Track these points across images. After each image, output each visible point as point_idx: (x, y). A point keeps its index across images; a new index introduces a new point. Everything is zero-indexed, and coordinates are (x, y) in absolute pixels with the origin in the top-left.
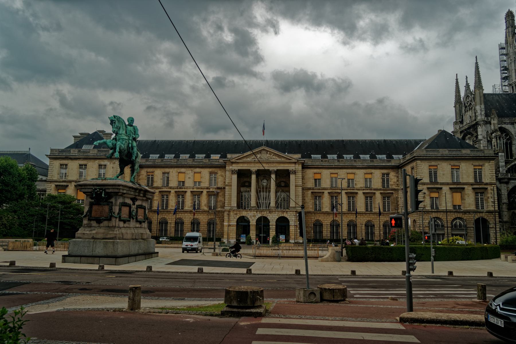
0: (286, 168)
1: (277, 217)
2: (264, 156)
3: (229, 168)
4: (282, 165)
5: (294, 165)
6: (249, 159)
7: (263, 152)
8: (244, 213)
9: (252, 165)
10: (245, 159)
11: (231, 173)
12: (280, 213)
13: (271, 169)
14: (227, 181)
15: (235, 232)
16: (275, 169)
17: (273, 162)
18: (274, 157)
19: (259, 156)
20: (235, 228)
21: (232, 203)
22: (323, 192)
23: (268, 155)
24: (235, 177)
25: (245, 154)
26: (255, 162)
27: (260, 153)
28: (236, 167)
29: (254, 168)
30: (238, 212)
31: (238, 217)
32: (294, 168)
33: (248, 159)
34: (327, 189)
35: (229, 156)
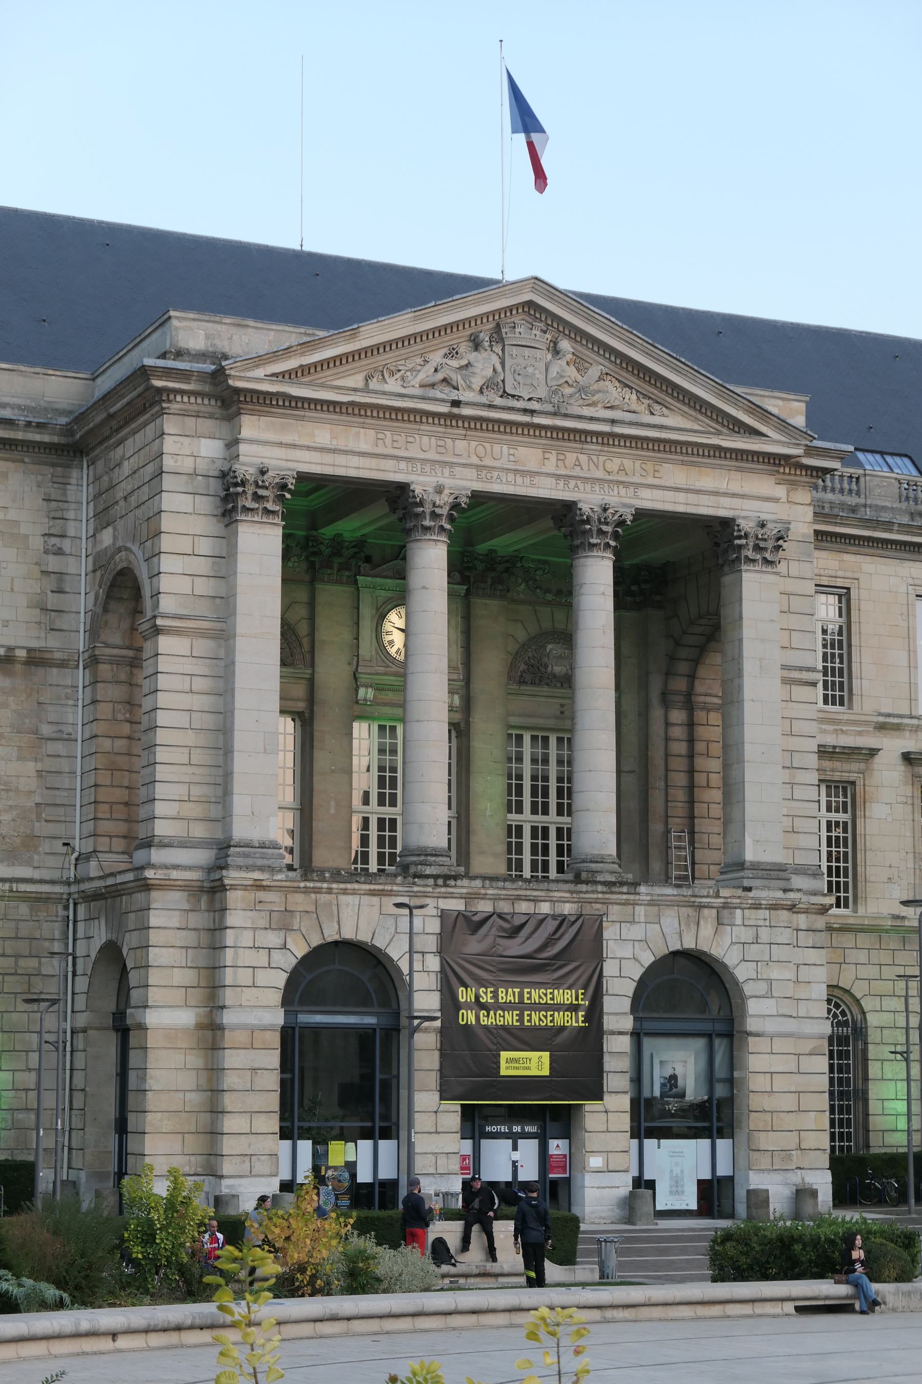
0: (706, 507)
1: (648, 959)
2: (537, 370)
3: (187, 446)
4: (674, 474)
5: (763, 484)
6: (391, 389)
7: (521, 331)
8: (361, 916)
9: (423, 443)
10: (356, 381)
11: (206, 504)
12: (670, 920)
13: (589, 500)
14: (177, 582)
15: (273, 1101)
16: (625, 501)
17: (607, 439)
18: (613, 391)
19: (484, 364)
20: (273, 1059)
21: (240, 803)
22: (873, 752)
23: (558, 366)
24: (261, 545)
25: (372, 333)
26: (452, 418)
27: (497, 335)
28: (276, 448)
29: (443, 470)
30: (299, 901)
31: (300, 950)
32: (767, 512)
33: (393, 385)
34: (897, 728)
35: (192, 332)
